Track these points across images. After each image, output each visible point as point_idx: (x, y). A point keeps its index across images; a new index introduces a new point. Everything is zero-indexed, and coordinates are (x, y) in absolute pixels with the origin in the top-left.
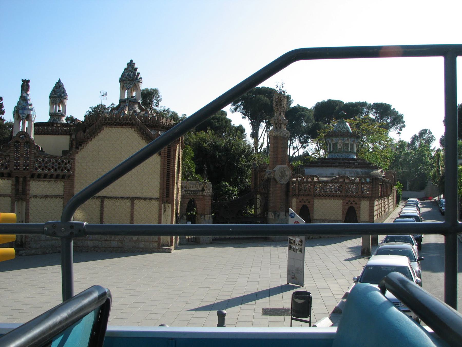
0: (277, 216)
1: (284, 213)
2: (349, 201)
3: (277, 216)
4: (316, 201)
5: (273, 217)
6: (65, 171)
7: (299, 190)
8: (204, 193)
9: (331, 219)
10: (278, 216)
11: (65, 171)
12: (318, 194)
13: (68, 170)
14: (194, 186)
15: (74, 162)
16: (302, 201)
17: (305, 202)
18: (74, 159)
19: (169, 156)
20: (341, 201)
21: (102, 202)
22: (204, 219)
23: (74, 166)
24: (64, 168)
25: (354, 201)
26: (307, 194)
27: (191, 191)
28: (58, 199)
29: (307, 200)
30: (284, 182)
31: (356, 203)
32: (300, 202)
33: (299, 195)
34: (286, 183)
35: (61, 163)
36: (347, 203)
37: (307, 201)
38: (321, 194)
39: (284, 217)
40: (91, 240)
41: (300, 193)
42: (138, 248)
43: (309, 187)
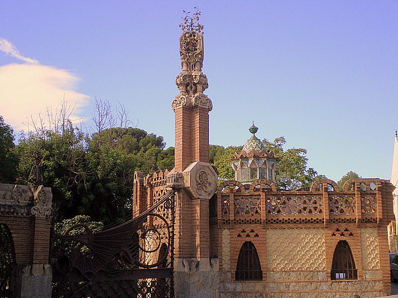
5: (186, 270)
8: (33, 212)
16: (241, 234)
17: (248, 236)
32: (239, 236)
33: (237, 222)
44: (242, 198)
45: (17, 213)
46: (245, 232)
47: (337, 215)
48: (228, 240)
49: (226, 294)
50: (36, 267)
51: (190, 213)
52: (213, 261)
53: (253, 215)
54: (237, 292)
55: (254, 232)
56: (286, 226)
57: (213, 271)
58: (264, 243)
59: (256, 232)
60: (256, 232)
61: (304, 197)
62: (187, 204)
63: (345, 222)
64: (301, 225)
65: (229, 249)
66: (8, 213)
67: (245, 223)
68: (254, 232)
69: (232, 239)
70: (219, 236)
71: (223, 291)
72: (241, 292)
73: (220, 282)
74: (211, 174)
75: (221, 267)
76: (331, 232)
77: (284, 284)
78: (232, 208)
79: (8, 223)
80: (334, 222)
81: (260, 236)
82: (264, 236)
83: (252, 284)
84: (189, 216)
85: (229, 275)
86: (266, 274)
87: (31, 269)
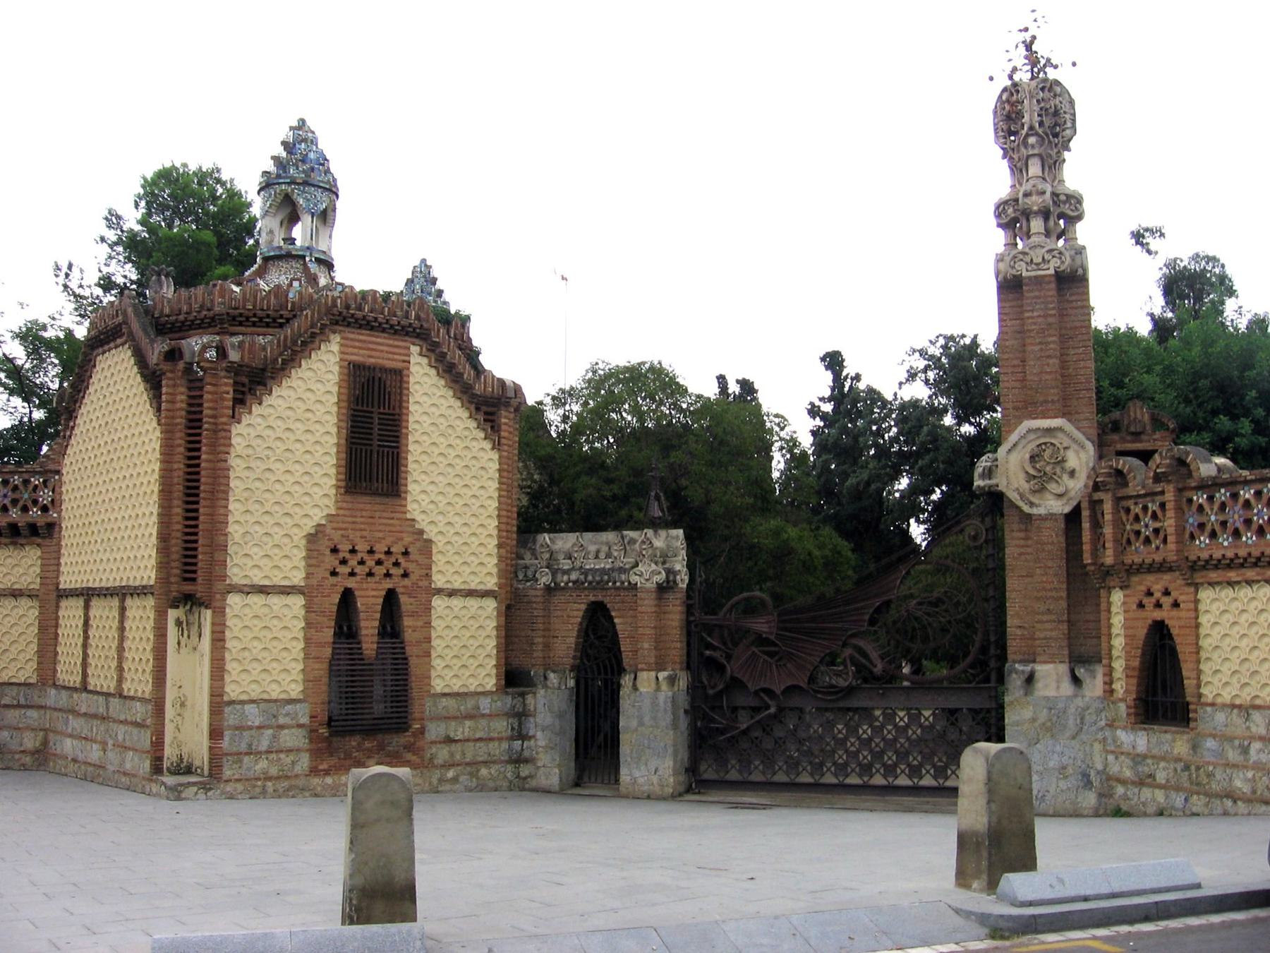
1: (1063, 668)
4: (1206, 595)
6: (35, 512)
7: (1124, 544)
8: (634, 579)
11: (35, 512)
12: (1205, 555)
13: (45, 509)
14: (605, 549)
15: (60, 480)
16: (1146, 601)
17: (1158, 605)
18: (58, 472)
19: (194, 422)
21: (87, 607)
22: (635, 688)
23: (61, 493)
24: (29, 504)
27: (586, 573)
28: (25, 602)
30: (1053, 505)
33: (1135, 570)
34: (1067, 510)
35: (21, 488)
39: (1067, 688)
40: (71, 736)
41: (1128, 561)
42: (125, 774)
44: (1136, 504)
45: (615, 583)
48: (1120, 619)
49: (1117, 758)
50: (643, 676)
53: (1157, 548)
62: (1020, 531)
66: (598, 583)
70: (1103, 606)
71: (1113, 748)
72: (1145, 757)
77: (1237, 742)
79: (606, 600)
83: (1168, 736)
84: (1026, 560)
85: (1122, 706)
86: (1196, 711)
87: (635, 678)
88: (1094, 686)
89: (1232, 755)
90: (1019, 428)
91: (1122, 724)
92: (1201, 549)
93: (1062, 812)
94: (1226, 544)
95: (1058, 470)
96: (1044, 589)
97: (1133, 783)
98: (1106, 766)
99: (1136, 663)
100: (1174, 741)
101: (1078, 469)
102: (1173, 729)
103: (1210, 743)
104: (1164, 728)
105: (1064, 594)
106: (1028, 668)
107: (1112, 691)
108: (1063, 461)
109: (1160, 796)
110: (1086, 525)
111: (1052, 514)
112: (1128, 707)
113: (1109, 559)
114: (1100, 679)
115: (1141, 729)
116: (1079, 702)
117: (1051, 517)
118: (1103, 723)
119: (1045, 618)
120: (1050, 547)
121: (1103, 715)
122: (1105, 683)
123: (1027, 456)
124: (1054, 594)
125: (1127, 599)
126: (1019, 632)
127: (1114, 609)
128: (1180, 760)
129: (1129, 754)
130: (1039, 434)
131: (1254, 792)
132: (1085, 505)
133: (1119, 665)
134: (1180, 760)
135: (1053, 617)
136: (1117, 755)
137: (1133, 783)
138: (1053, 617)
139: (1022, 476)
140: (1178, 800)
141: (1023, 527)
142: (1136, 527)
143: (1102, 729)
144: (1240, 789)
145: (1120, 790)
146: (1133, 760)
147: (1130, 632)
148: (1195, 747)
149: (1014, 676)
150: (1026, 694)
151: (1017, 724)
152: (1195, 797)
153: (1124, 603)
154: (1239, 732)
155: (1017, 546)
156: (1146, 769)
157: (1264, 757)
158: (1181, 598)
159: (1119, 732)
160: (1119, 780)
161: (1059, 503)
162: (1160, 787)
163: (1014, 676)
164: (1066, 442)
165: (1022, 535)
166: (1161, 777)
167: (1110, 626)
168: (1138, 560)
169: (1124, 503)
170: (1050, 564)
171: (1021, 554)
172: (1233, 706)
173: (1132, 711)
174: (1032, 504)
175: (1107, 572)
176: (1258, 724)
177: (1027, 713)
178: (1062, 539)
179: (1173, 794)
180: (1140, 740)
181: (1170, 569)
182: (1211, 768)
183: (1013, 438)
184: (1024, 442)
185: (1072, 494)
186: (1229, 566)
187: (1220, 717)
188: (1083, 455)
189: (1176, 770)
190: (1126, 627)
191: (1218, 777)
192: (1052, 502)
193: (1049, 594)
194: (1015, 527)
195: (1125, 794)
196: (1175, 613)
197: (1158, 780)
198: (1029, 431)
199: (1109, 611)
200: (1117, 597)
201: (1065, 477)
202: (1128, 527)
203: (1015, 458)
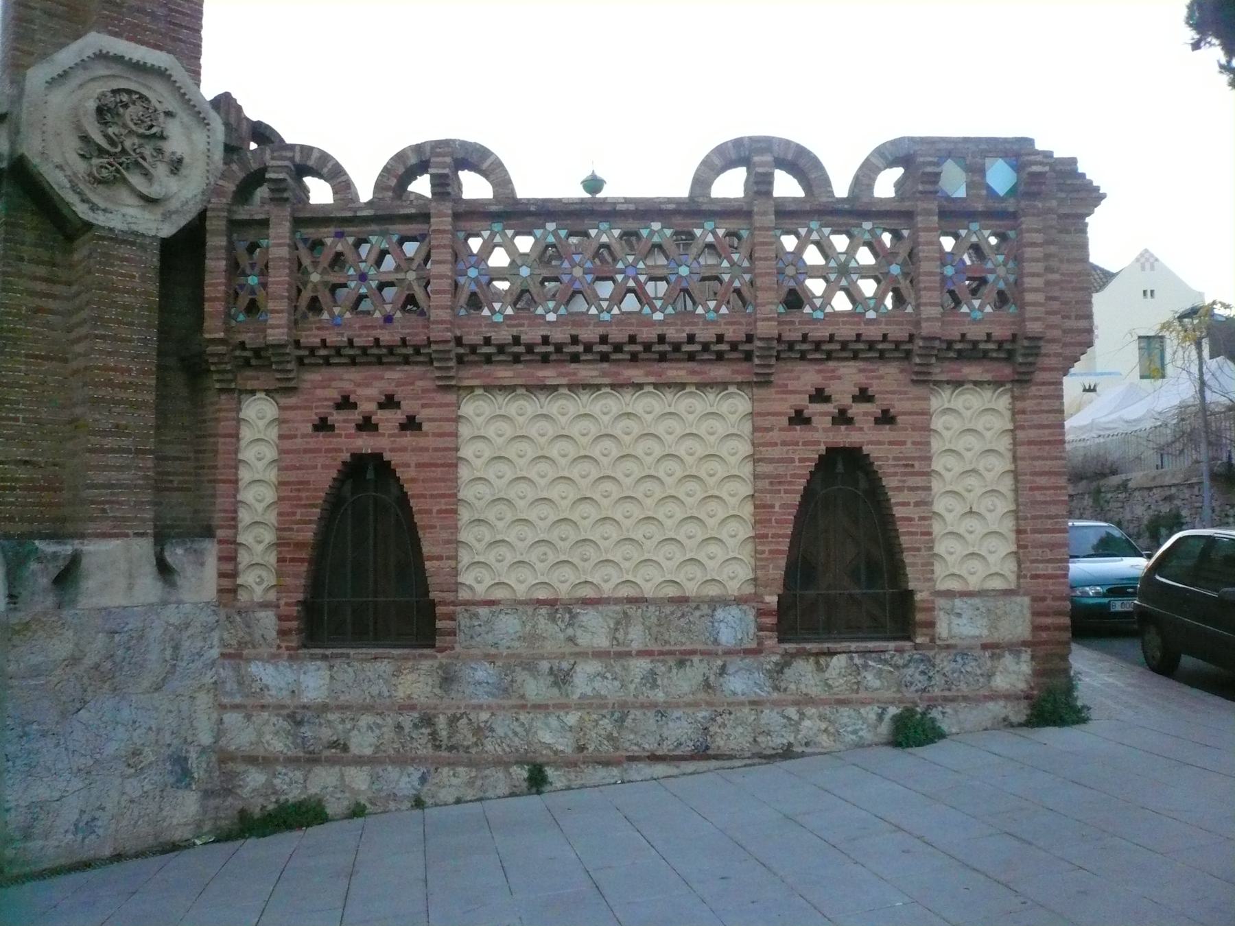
0: (39, 576)
2: (820, 396)
3: (39, 576)
4: (476, 410)
9: (648, 591)
10: (67, 577)
12: (504, 336)
16: (336, 417)
17: (367, 425)
20: (737, 405)
25: (863, 396)
26: (386, 337)
29: (389, 402)
30: (135, 216)
31: (886, 418)
32: (323, 426)
34: (167, 231)
36: (799, 419)
37: (388, 420)
38: (531, 335)
39: (148, 587)
41: (311, 338)
43: (404, 263)
44: (340, 235)
46: (354, 406)
47: (817, 320)
48: (263, 450)
49: (248, 717)
51: (52, 304)
52: (176, 555)
53: (388, 319)
54: (304, 707)
55: (397, 405)
56: (561, 375)
57: (179, 602)
58: (451, 463)
59: (409, 406)
60: (409, 406)
61: (656, 226)
62: (39, 262)
63: (855, 356)
64: (635, 373)
65: (270, 495)
67: (353, 362)
68: (397, 405)
69: (288, 444)
70: (224, 427)
71: (238, 700)
72: (325, 708)
73: (223, 655)
74: (183, 115)
75: (227, 583)
76: (786, 406)
77: (544, 666)
78: (280, 278)
80: (803, 357)
81: (425, 427)
82: (448, 427)
83: (384, 667)
85: (267, 621)
86: (451, 617)
88: (200, 579)
89: (535, 688)
90: (80, 43)
91: (264, 651)
92: (496, 324)
93: (130, 846)
94: (551, 317)
95: (148, 151)
96: (110, 383)
97: (292, 761)
98: (219, 733)
99: (308, 534)
100: (397, 673)
101: (187, 160)
102: (396, 652)
103: (484, 672)
104: (374, 651)
105: (150, 398)
106: (67, 549)
107: (234, 591)
108: (162, 137)
109: (359, 779)
110: (216, 264)
111: (136, 234)
112: (281, 618)
113: (277, 329)
114: (211, 566)
115: (313, 658)
116: (172, 615)
117: (131, 238)
118: (215, 653)
119: (109, 442)
120: (127, 299)
121: (216, 635)
122: (222, 575)
123: (92, 105)
124: (129, 394)
125: (290, 415)
126: (22, 473)
127: (246, 434)
128: (413, 708)
129: (283, 707)
130: (116, 69)
131: (581, 749)
132: (215, 224)
133: (257, 541)
134: (413, 708)
135: (126, 442)
136: (247, 711)
137: (292, 761)
138: (126, 442)
139: (72, 144)
140: (405, 782)
141: (46, 256)
142: (334, 278)
143: (213, 663)
144: (548, 746)
145: (255, 778)
146: (291, 717)
147: (292, 476)
148: (447, 680)
149: (34, 566)
150: (60, 606)
151: (36, 672)
152: (445, 771)
153: (280, 421)
154: (549, 647)
155: (32, 293)
156: (326, 734)
157: (608, 688)
158: (422, 414)
159: (255, 669)
160: (252, 760)
161: (147, 216)
162: (359, 761)
163: (34, 566)
164: (171, 104)
165: (42, 271)
166: (362, 743)
167: (236, 464)
168: (333, 338)
169: (311, 233)
170: (124, 333)
171: (38, 310)
172: (540, 603)
173: (294, 624)
174: (94, 208)
175: (259, 358)
176: (595, 630)
177: (61, 647)
178: (154, 288)
179: (392, 772)
180: (314, 680)
181: (406, 361)
182: (484, 716)
183: (67, 56)
184: (82, 76)
185: (174, 204)
186: (545, 359)
187: (509, 624)
188: (199, 137)
189: (399, 727)
190: (281, 464)
191: (500, 731)
192: (131, 211)
193: (121, 395)
194: (27, 251)
195: (269, 784)
196: (408, 439)
197: (354, 750)
198: (102, 57)
199: (236, 436)
200: (259, 413)
201: (161, 170)
202: (315, 277)
203: (59, 100)
